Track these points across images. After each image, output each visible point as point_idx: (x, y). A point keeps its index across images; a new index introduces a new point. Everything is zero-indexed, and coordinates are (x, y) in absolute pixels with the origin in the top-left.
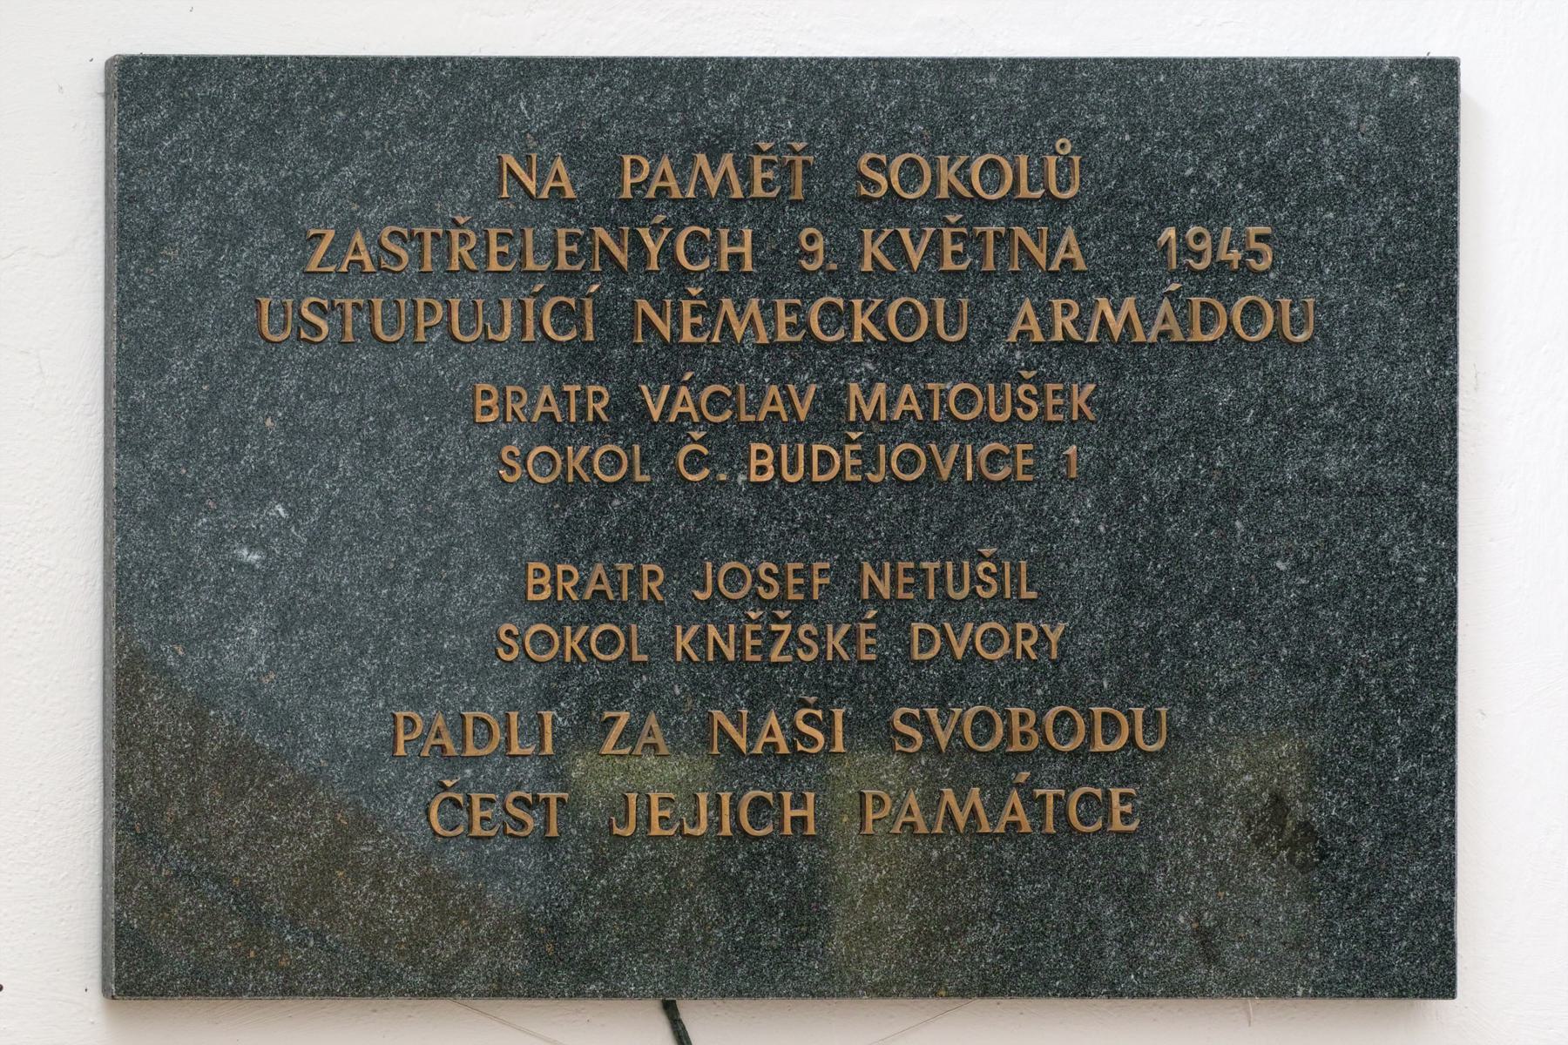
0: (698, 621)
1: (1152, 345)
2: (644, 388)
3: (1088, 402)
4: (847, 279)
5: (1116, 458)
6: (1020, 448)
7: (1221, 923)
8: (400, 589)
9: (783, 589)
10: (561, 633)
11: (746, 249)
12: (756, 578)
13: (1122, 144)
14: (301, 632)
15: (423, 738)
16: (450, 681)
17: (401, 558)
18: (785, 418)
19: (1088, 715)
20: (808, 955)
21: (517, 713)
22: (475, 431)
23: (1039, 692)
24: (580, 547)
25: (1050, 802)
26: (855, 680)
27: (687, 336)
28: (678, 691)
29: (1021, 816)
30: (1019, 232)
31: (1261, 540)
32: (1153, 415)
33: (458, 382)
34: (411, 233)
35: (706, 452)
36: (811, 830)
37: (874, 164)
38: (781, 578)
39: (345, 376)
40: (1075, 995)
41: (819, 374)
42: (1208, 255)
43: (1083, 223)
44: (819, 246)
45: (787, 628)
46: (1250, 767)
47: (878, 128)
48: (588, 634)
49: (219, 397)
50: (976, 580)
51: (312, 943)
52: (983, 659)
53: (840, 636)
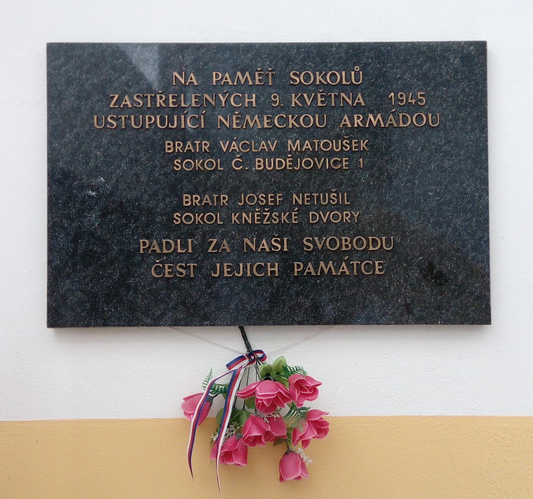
0: (240, 212)
1: (387, 128)
2: (221, 142)
3: (366, 145)
4: (287, 109)
5: (376, 162)
6: (344, 159)
7: (413, 301)
8: (142, 203)
9: (267, 202)
10: (194, 216)
11: (254, 100)
12: (258, 199)
13: (377, 68)
14: (109, 216)
15: (149, 247)
16: (159, 231)
17: (142, 194)
18: (267, 151)
19: (367, 240)
20: (277, 312)
21: (180, 240)
22: (166, 155)
23: (352, 232)
24: (201, 190)
25: (355, 265)
26: (292, 229)
27: (235, 126)
28: (233, 233)
29: (346, 270)
30: (343, 94)
31: (424, 186)
32: (388, 149)
33: (160, 141)
34: (143, 96)
35: (241, 161)
36: (277, 274)
37: (295, 74)
38: (266, 198)
39: (123, 139)
40: (365, 324)
41: (278, 138)
42: (405, 100)
43: (364, 92)
44: (277, 99)
45: (268, 214)
46: (421, 255)
47: (297, 64)
48: (203, 216)
49: (82, 145)
50: (330, 199)
51: (113, 310)
52: (333, 222)
53: (286, 216)
